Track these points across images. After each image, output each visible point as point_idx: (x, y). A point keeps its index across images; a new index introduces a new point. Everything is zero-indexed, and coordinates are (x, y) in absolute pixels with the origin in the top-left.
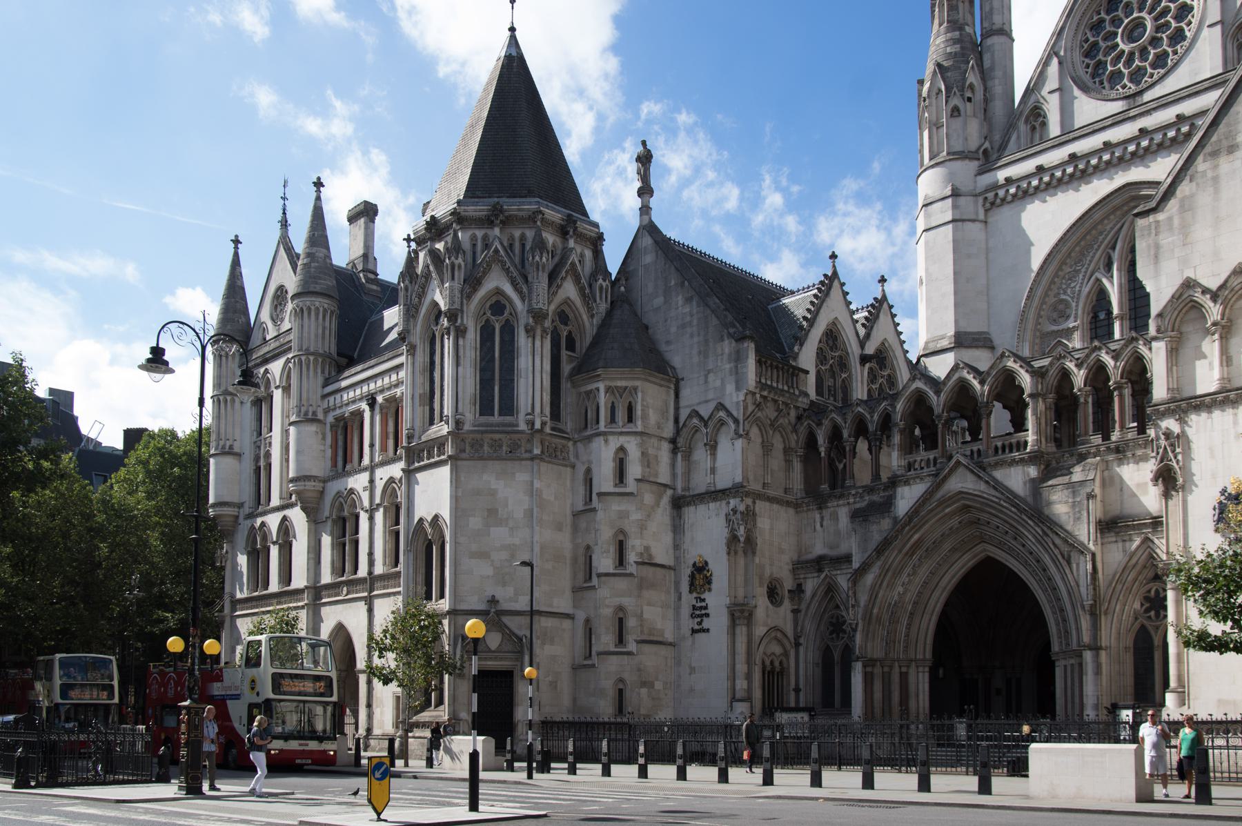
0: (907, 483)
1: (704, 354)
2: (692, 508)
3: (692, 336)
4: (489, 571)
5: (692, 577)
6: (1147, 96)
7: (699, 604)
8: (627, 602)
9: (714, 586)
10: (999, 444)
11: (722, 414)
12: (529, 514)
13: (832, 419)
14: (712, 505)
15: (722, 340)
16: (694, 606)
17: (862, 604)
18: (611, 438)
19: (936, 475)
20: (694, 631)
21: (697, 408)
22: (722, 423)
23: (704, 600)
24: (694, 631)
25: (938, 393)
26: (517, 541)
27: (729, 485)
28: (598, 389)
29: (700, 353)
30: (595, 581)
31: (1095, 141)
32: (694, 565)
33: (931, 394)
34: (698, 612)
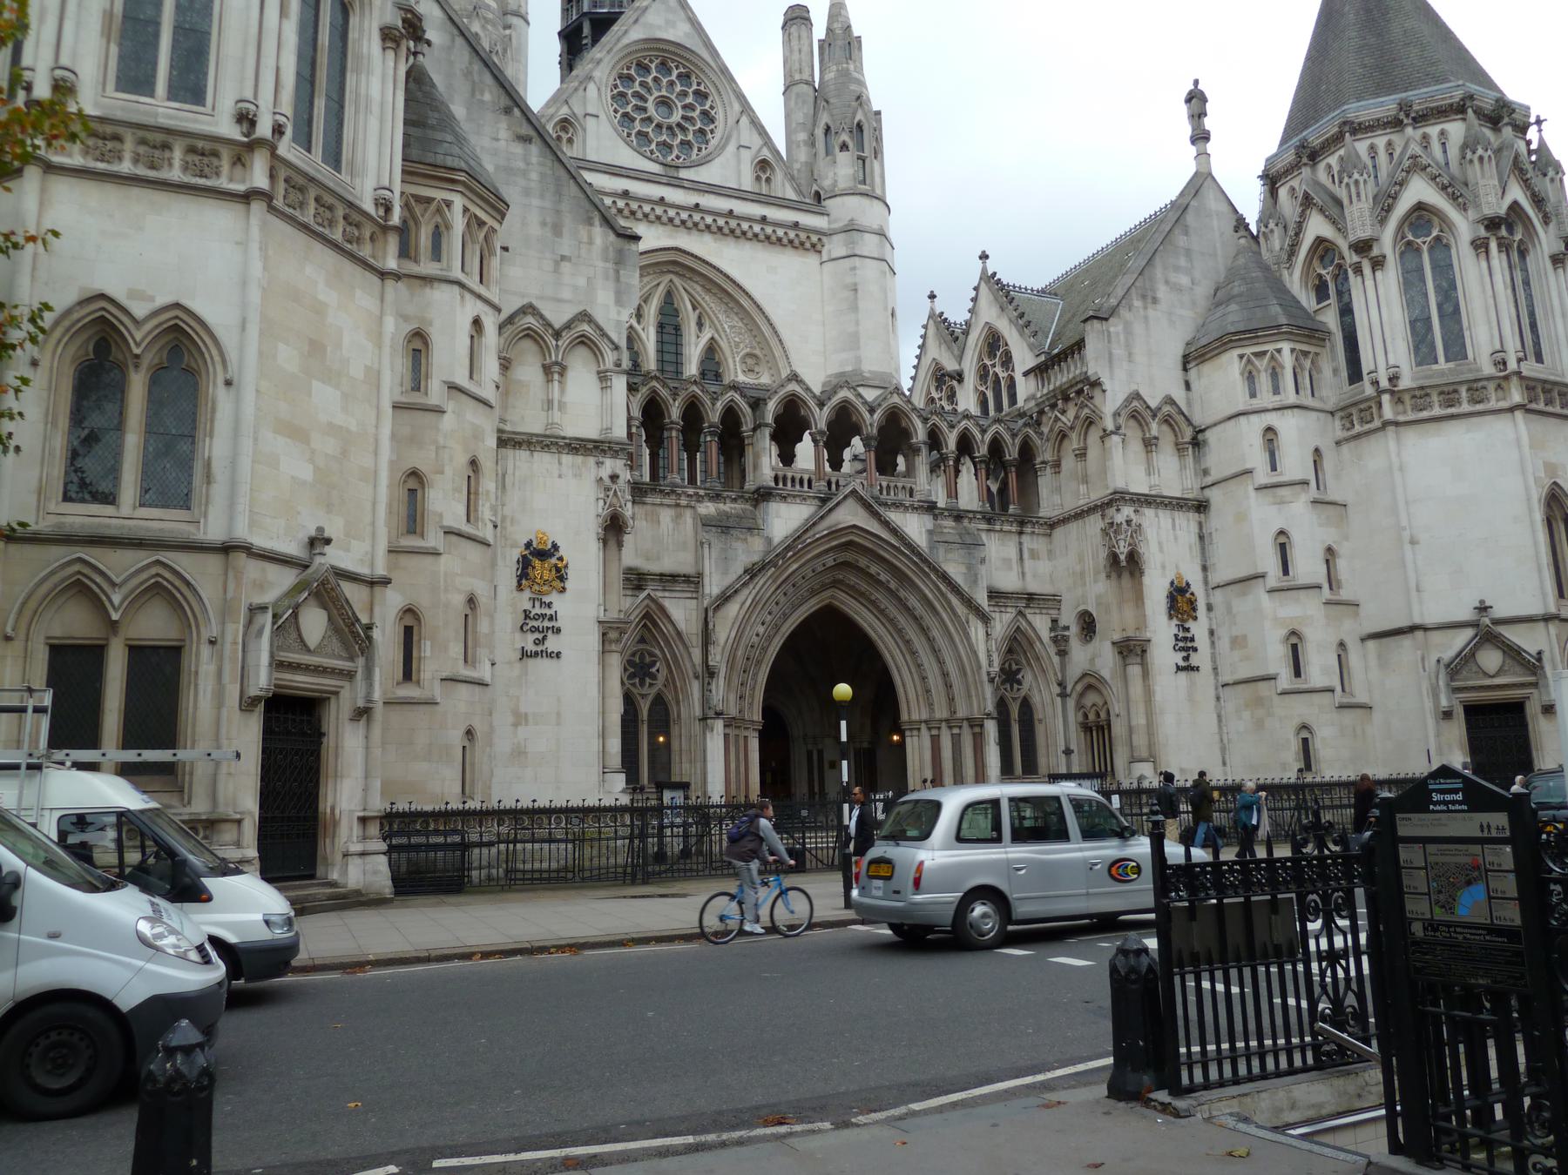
0: (784, 498)
1: (557, 230)
2: (523, 454)
3: (527, 192)
4: (306, 472)
5: (525, 565)
6: (683, 174)
7: (537, 610)
8: (481, 590)
9: (568, 585)
10: (884, 484)
11: (585, 327)
12: (374, 377)
13: (654, 391)
14: (567, 459)
15: (589, 222)
16: (527, 614)
17: (722, 641)
18: (468, 296)
19: (824, 501)
20: (525, 654)
21: (536, 303)
22: (583, 341)
23: (549, 605)
24: (525, 654)
25: (821, 405)
26: (353, 428)
27: (592, 433)
28: (449, 204)
29: (544, 224)
30: (434, 539)
31: (655, 191)
32: (528, 545)
33: (812, 403)
34: (535, 624)
